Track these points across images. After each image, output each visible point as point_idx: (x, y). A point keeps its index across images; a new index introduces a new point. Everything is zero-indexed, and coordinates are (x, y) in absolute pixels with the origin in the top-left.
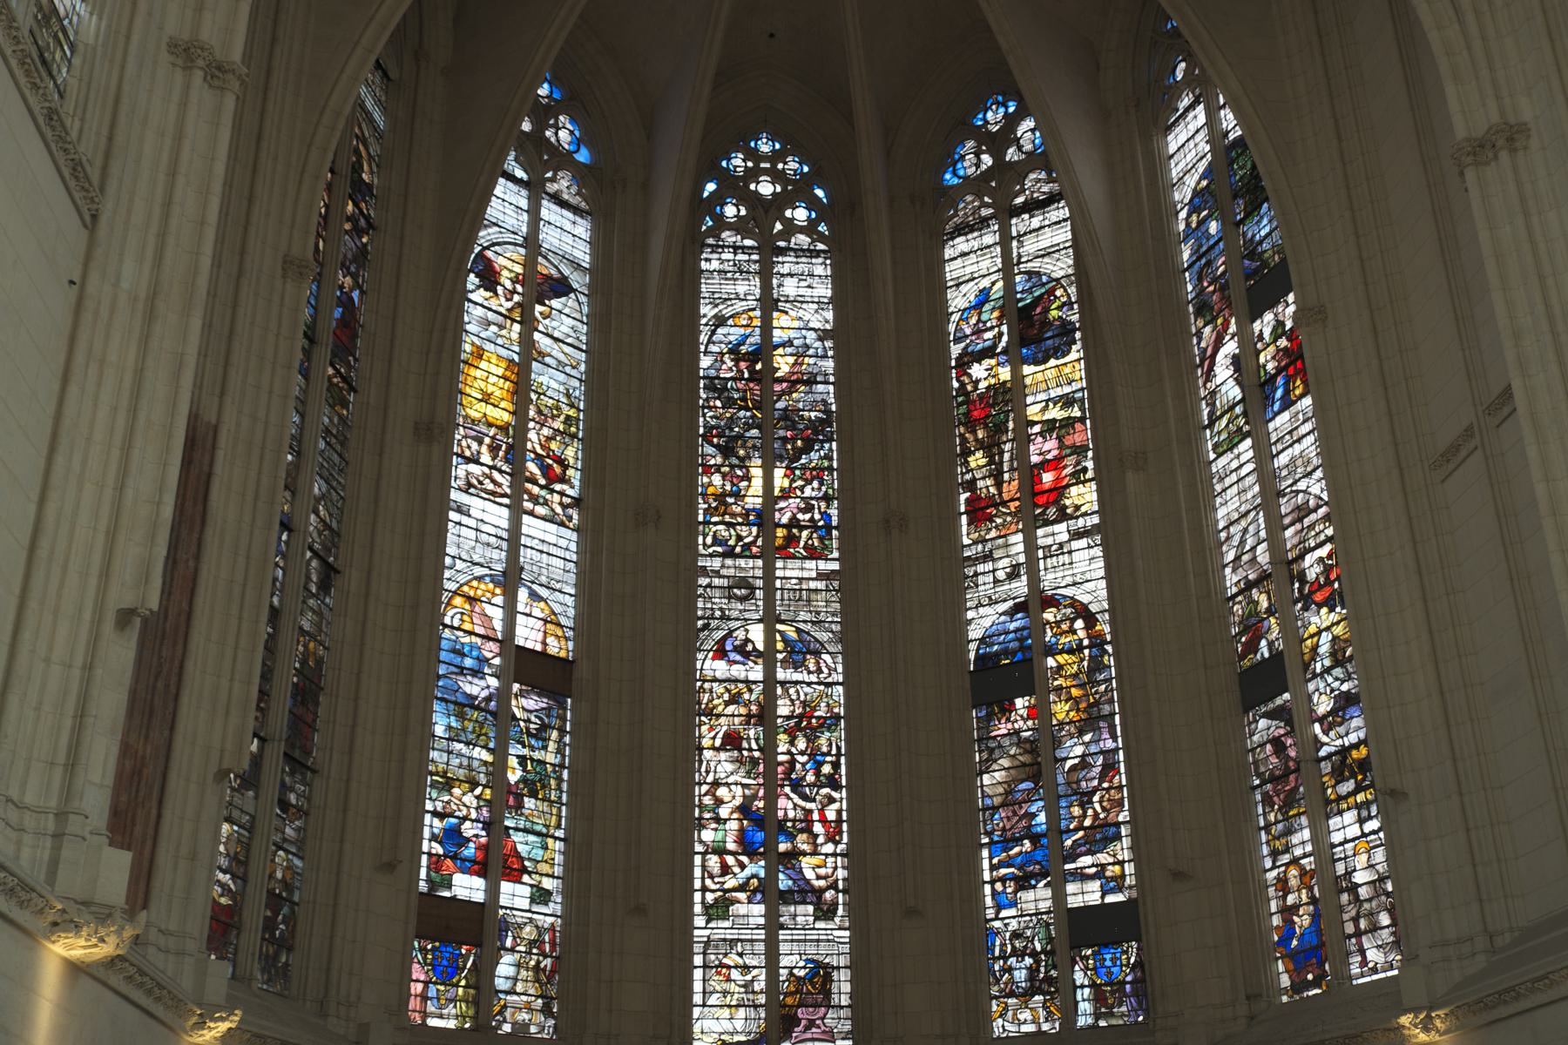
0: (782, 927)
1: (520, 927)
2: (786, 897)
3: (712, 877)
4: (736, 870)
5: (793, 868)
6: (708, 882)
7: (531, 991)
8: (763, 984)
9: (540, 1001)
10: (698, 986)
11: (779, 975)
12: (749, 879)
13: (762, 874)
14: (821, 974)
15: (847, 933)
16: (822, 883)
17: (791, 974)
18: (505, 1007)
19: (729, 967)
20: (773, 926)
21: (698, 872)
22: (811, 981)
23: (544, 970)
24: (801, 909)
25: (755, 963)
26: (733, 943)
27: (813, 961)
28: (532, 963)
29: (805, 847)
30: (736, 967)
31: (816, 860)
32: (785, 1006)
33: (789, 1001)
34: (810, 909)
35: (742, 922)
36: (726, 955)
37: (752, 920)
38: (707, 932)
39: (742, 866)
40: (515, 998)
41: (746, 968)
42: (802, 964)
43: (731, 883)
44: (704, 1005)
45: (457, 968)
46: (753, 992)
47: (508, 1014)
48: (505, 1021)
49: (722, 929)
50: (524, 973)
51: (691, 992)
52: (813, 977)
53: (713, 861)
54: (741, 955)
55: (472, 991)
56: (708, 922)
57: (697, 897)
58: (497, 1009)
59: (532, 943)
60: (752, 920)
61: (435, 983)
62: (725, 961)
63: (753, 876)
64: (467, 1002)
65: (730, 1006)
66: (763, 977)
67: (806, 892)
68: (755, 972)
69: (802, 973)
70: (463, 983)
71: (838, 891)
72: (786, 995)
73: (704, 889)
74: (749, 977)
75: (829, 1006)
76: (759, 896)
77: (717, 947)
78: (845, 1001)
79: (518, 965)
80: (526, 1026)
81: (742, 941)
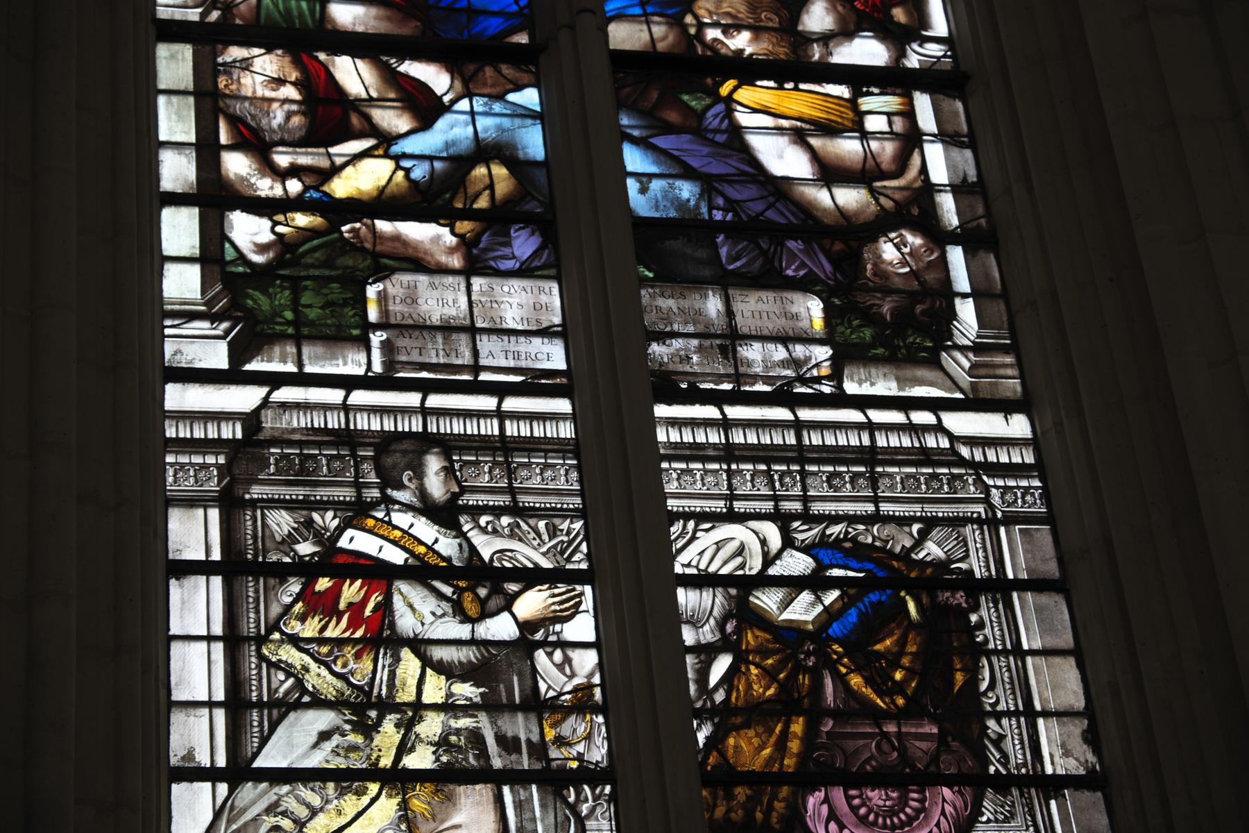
0: (670, 387)
2: (674, 251)
3: (256, 143)
4: (393, 120)
5: (694, 126)
6: (237, 164)
8: (586, 661)
10: (196, 672)
11: (675, 618)
12: (460, 163)
13: (533, 142)
14: (905, 623)
15: (1019, 426)
16: (850, 197)
17: (743, 614)
19: (377, 573)
20: (613, 381)
21: (175, 122)
22: (859, 648)
24: (754, 308)
25: (530, 554)
26: (396, 454)
27: (853, 552)
29: (742, 42)
30: (423, 571)
31: (800, 101)
32: (726, 777)
33: (750, 749)
34: (813, 310)
35: (432, 359)
36: (356, 514)
37: (492, 351)
38: (245, 398)
39: (426, 109)
41: (478, 584)
42: (797, 564)
43: (364, 177)
44: (238, 771)
46: (536, 705)
49: (328, 386)
51: (160, 704)
52: (871, 627)
53: (262, 74)
54: (444, 514)
56: (239, 353)
57: (179, 230)
60: (492, 351)
62: (359, 541)
63: (484, 151)
65: (397, 779)
66: (582, 628)
67: (779, 234)
68: (532, 603)
69: (803, 610)
71: (938, 237)
72: (727, 718)
73: (214, 198)
74: (501, 628)
75: (977, 782)
76: (524, 245)
77: (302, 473)
78: (1060, 750)
81: (447, 445)
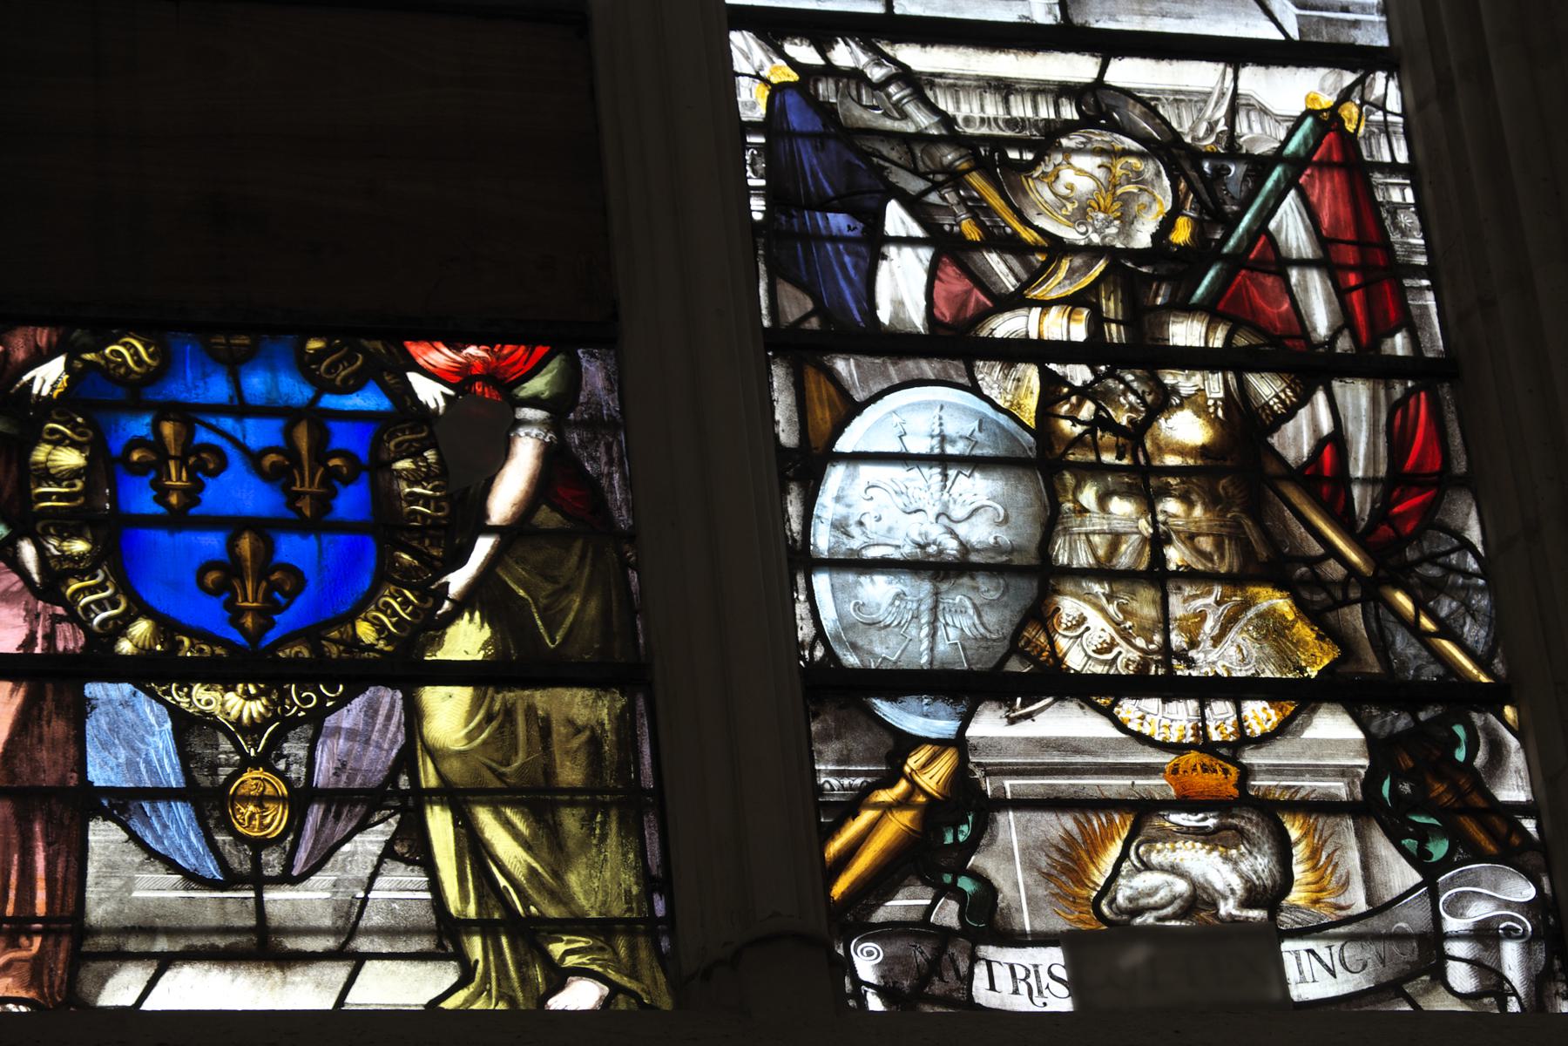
1: (1006, 160)
7: (1216, 660)
9: (1333, 728)
18: (968, 803)
23: (1325, 471)
28: (1186, 430)
40: (1064, 722)
45: (388, 523)
47: (1011, 859)
48: (988, 923)
50: (1108, 519)
55: (578, 706)
58: (877, 831)
59: (1137, 284)
61: (147, 672)
64: (536, 799)
70: (466, 640)
79: (1040, 462)
80: (1230, 951)
